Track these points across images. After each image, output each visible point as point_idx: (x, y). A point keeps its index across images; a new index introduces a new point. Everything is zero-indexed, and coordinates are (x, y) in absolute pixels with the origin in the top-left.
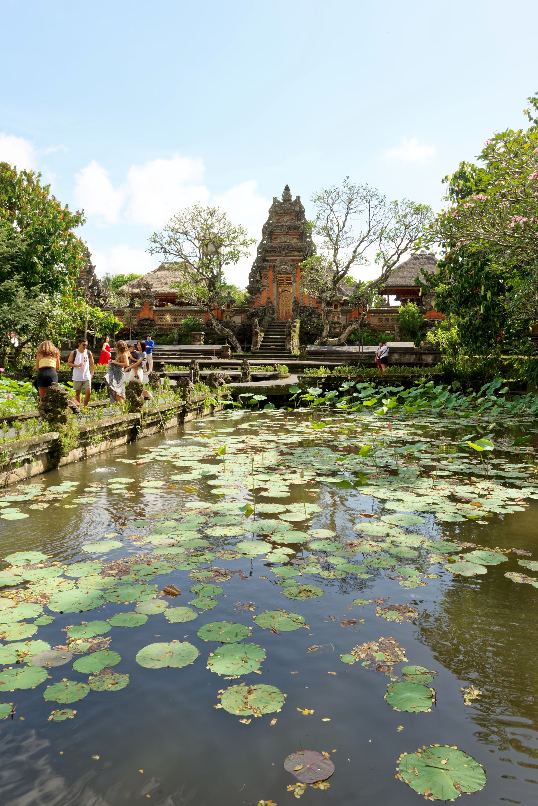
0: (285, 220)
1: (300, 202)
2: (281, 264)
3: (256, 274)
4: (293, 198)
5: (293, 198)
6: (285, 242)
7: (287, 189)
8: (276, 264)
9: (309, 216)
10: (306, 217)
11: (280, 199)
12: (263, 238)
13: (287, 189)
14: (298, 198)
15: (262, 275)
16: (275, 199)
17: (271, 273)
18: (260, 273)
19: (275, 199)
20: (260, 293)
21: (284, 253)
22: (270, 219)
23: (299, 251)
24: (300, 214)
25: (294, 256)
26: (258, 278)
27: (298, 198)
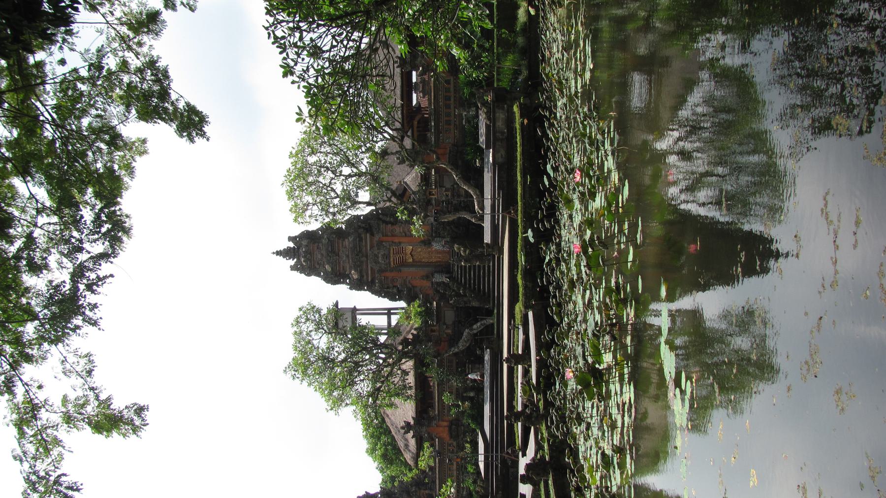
0: (319, 256)
1: (295, 237)
2: (377, 262)
3: (388, 292)
4: (291, 245)
5: (291, 245)
6: (348, 256)
7: (278, 253)
8: (376, 268)
9: (314, 226)
10: (315, 229)
11: (292, 262)
12: (343, 283)
13: (278, 253)
14: (291, 239)
15: (391, 285)
16: (293, 268)
17: (388, 274)
18: (388, 288)
19: (293, 268)
20: (414, 287)
21: (364, 259)
22: (318, 275)
23: (361, 240)
24: (308, 237)
25: (366, 246)
26: (395, 290)
27: (291, 239)
